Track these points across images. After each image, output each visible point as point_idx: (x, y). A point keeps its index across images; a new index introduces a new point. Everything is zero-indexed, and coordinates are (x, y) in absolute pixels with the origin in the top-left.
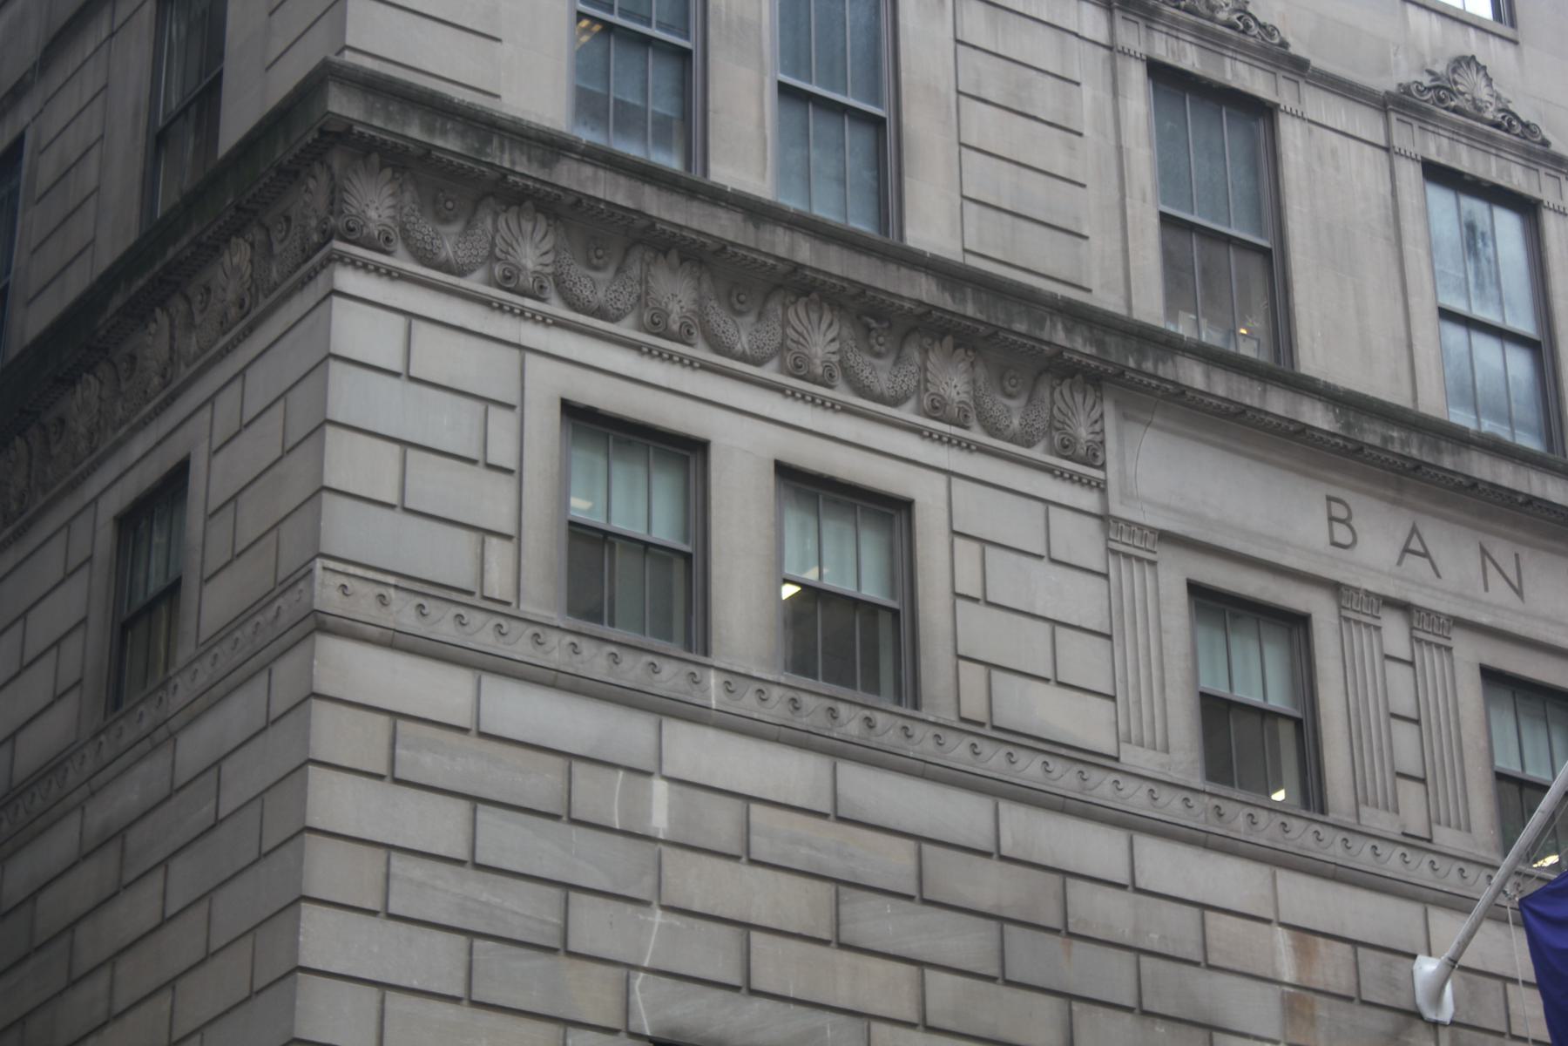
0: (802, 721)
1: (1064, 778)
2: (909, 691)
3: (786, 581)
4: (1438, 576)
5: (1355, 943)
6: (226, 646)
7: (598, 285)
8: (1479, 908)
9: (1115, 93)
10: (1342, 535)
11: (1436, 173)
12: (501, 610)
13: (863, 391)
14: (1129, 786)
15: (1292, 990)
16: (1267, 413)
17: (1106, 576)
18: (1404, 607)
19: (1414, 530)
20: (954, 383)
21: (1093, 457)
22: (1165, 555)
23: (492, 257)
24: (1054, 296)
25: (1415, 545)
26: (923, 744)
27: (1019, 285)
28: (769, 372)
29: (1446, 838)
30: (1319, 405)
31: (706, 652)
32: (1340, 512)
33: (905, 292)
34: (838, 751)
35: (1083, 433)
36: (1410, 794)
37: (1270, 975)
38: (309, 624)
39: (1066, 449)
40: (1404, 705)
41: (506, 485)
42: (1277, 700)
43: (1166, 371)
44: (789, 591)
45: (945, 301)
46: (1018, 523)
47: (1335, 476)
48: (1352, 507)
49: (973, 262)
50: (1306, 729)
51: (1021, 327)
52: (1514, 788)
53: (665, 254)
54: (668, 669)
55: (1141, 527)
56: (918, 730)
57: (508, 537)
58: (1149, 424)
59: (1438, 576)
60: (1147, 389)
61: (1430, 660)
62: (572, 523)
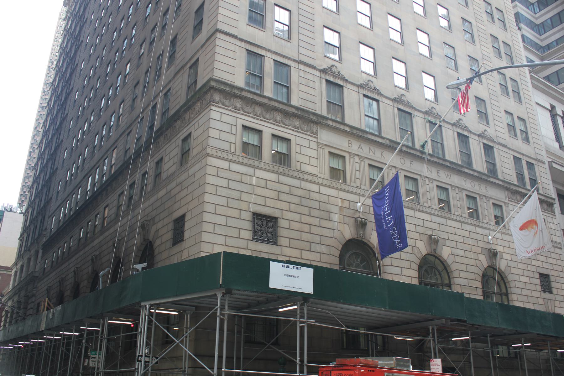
0: (274, 169)
1: (310, 178)
2: (289, 166)
3: (273, 150)
6: (196, 158)
7: (248, 109)
9: (321, 84)
10: (350, 145)
12: (233, 153)
13: (284, 124)
14: (319, 179)
17: (317, 150)
18: (358, 155)
19: (360, 145)
20: (297, 123)
21: (316, 134)
22: (325, 147)
23: (233, 105)
25: (360, 147)
26: (291, 173)
27: (306, 110)
28: (271, 121)
29: (363, 187)
31: (261, 160)
32: (350, 142)
33: (290, 111)
34: (279, 174)
35: (315, 131)
36: (358, 181)
38: (207, 155)
39: (312, 133)
40: (358, 169)
41: (234, 136)
42: (341, 168)
43: (326, 122)
44: (273, 152)
45: (296, 112)
46: (305, 143)
47: (349, 137)
49: (300, 107)
50: (344, 172)
51: (306, 116)
52: (372, 180)
53: (257, 105)
54: (256, 162)
56: (290, 171)
61: (362, 163)
62: (243, 142)
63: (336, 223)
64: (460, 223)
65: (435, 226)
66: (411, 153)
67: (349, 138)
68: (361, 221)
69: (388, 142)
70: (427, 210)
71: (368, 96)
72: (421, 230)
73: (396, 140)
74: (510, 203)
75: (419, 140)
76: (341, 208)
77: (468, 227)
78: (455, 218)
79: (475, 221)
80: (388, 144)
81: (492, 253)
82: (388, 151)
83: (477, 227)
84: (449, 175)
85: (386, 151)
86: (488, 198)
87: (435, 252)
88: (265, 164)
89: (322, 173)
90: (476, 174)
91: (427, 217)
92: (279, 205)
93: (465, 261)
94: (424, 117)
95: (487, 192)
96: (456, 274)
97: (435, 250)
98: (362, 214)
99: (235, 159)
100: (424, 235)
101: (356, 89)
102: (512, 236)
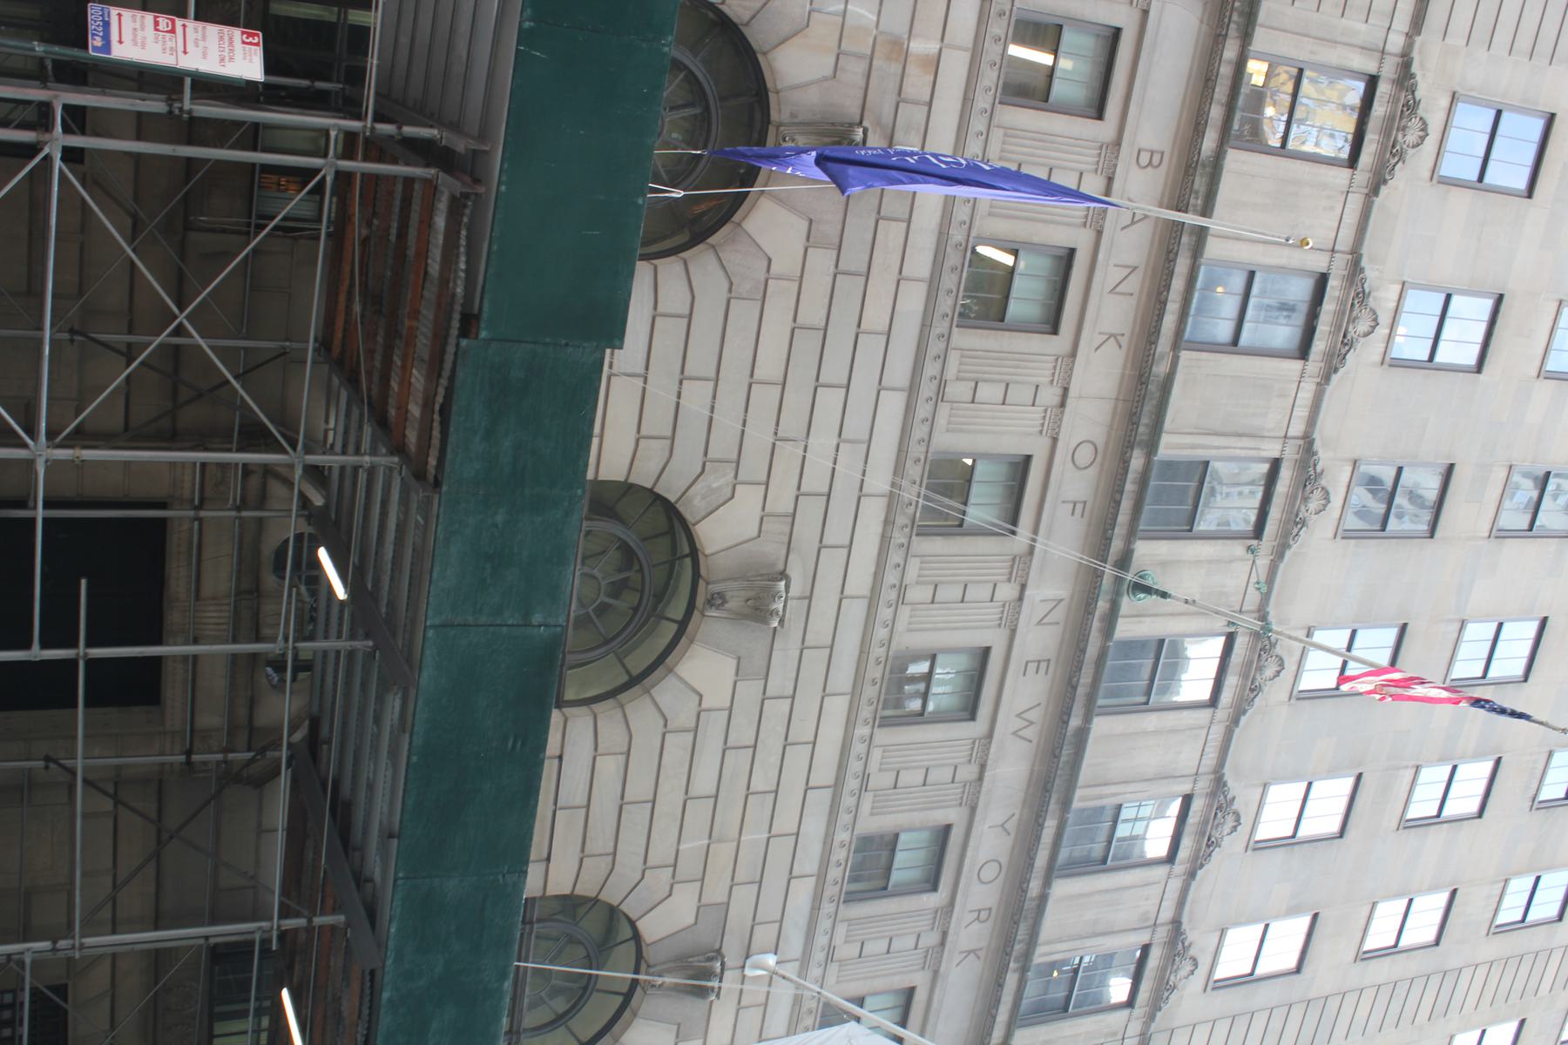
0: (909, 463)
3: (974, 461)
4: (1123, 229)
5: (930, 104)
8: (802, 982)
11: (1276, 464)
14: (929, 407)
15: (905, 46)
16: (1211, 104)
22: (1045, 442)
29: (833, 968)
36: (888, 779)
37: (913, 32)
40: (895, 945)
42: (896, 876)
44: (969, 462)
48: (1087, 471)
59: (1123, 229)
63: (842, 7)
64: (831, 781)
67: (1172, 153)
70: (891, 577)
72: (807, 530)
73: (1122, 617)
75: (1164, 564)
76: (899, 50)
77: (814, 827)
79: (837, 888)
80: (1154, 369)
81: (708, 964)
84: (1028, 733)
86: (933, 961)
87: (710, 602)
88: (925, 443)
89: (964, 367)
90: (1034, 887)
94: (1162, 925)
95: (958, 958)
96: (612, 731)
102: (788, 1035)
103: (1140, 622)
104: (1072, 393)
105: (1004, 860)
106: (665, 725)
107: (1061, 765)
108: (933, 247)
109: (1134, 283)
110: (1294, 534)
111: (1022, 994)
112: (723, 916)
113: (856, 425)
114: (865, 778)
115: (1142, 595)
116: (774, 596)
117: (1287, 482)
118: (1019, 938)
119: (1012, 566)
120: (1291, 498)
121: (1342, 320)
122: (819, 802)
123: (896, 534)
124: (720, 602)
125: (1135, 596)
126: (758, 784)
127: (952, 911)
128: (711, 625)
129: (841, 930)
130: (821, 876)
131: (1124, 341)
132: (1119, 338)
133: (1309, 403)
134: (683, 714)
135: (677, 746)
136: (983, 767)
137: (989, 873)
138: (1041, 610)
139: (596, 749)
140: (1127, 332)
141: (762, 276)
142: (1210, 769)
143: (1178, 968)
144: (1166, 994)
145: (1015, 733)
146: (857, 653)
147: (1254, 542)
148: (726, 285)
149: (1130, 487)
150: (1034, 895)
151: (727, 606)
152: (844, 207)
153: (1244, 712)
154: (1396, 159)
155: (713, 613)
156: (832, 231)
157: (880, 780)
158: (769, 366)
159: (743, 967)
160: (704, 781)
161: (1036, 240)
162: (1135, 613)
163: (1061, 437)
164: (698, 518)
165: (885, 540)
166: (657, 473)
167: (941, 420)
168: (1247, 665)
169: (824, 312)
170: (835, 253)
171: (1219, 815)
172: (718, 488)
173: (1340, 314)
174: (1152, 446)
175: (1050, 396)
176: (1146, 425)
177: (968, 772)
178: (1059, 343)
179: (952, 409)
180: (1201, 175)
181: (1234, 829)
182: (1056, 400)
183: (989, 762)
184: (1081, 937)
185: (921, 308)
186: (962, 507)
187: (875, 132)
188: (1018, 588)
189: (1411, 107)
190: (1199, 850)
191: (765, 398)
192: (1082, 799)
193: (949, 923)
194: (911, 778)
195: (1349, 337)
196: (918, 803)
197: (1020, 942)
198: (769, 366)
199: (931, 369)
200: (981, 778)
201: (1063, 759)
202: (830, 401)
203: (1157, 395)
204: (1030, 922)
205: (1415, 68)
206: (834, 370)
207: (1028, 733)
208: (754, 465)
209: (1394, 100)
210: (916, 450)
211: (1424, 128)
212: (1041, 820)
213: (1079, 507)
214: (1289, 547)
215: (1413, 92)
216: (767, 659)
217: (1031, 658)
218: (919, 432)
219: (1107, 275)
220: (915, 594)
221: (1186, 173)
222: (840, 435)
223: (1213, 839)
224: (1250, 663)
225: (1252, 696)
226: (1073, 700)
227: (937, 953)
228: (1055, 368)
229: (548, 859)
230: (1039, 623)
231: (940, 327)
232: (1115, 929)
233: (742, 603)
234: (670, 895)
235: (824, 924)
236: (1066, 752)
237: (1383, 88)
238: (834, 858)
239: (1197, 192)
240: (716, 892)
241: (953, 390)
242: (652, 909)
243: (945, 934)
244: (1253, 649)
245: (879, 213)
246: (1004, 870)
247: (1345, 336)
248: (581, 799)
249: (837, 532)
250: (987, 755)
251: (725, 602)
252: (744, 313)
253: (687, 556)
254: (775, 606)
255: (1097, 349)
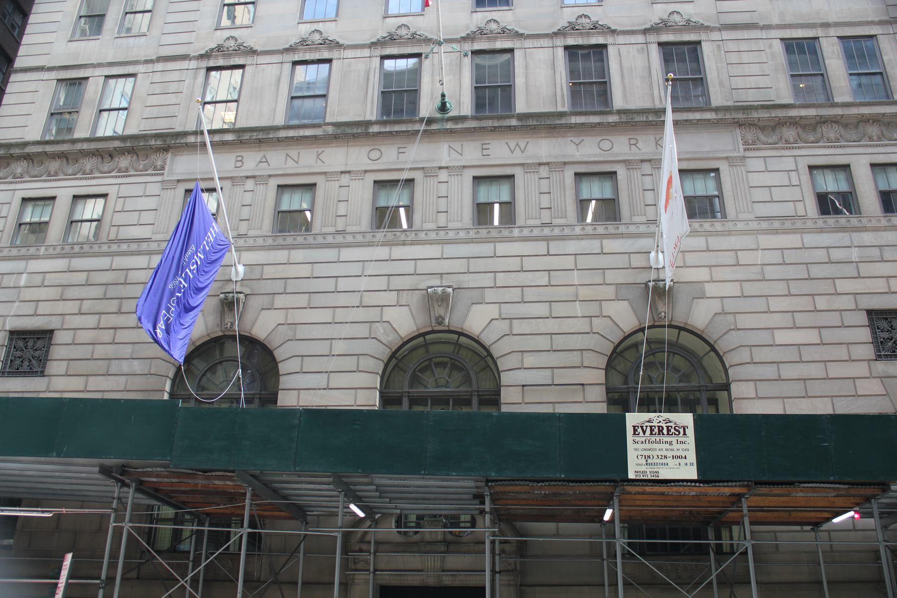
1: (134, 247)
7: (37, 170)
10: (239, 164)
12: (804, 218)
19: (287, 155)
20: (124, 162)
24: (152, 134)
27: (166, 133)
30: (230, 134)
32: (240, 158)
35: (159, 163)
39: (155, 169)
43: (183, 141)
45: (122, 145)
47: (238, 150)
50: (720, 197)
51: (141, 144)
52: (601, 202)
54: (610, 227)
55: (171, 180)
57: (801, 201)
58: (183, 155)
60: (178, 147)
61: (261, 188)
65: (460, 266)
66: (397, 132)
68: (226, 298)
69: (330, 130)
71: (306, 60)
74: (748, 154)
78: (526, 232)
82: (336, 147)
83: (853, 231)
84: (522, 146)
85: (333, 147)
91: (433, 251)
92: (61, 307)
93: (551, 326)
97: (440, 320)
98: (242, 285)
99: (810, 224)
100: (411, 292)
101: (366, 52)
103: (463, 103)
104: (344, 170)
105: (599, 139)
106: (508, 335)
107: (539, 123)
108: (275, 251)
109: (293, 153)
110: (419, 37)
111: (681, 108)
112: (624, 285)
113: (355, 269)
114: (544, 225)
115: (448, 105)
116: (435, 293)
117: (393, 49)
118: (645, 119)
119: (429, 176)
120: (401, 44)
121: (314, 48)
122: (555, 247)
123: (410, 238)
124: (440, 319)
125: (449, 109)
126: (545, 281)
127: (628, 160)
128: (453, 320)
129: (636, 219)
130: (708, 234)
131: (320, 150)
132: (319, 153)
133: (353, 51)
134: (503, 326)
135: (518, 327)
136: (540, 164)
137: (606, 145)
138: (454, 155)
139: (520, 368)
140: (316, 150)
141: (285, 327)
142: (550, 41)
143: (675, 22)
144: (692, 24)
145: (523, 152)
146: (472, 244)
147: (423, 56)
148: (289, 342)
149: (388, 129)
150: (618, 118)
151: (442, 314)
152: (257, 296)
153: (517, 32)
154: (241, 47)
155: (447, 321)
156: (266, 299)
157: (546, 217)
158: (325, 316)
159: (658, 269)
160: (542, 309)
161: (273, 204)
162: (458, 107)
163: (364, 169)
164: (398, 337)
165: (413, 243)
166: (375, 359)
167: (355, 229)
168: (489, 39)
169: (302, 295)
170: (276, 296)
171: (577, 28)
172: (384, 329)
173: (310, 50)
174: (369, 123)
175: (345, 180)
176: (357, 130)
177: (544, 171)
178: (319, 180)
179: (425, 222)
180: (244, 136)
181: (586, 16)
182: (347, 175)
183: (538, 161)
184: (651, 84)
185: (301, 251)
186: (390, 209)
187: (225, 288)
188: (442, 170)
189: (219, 48)
190: (598, 32)
191: (341, 315)
192: (563, 106)
193: (635, 160)
194: (545, 201)
195: (321, 42)
196: (561, 193)
197: (647, 118)
198: (325, 316)
199: (330, 239)
200: (548, 164)
201: (535, 123)
202: (343, 284)
203: (343, 128)
204: (635, 115)
205: (203, 52)
206: (329, 285)
207: (522, 146)
208: (373, 314)
209: (216, 57)
210: (472, 234)
211: (228, 39)
212: (573, 125)
213: (401, 150)
214: (426, 37)
215: (213, 49)
216: (473, 290)
217: (481, 154)
218: (359, 238)
219: (290, 167)
220: (442, 223)
221: (244, 143)
222: (361, 276)
223: (592, 27)
224: (489, 38)
225: (507, 31)
226: (501, 127)
227: (655, 162)
228: (331, 180)
229: (583, 385)
230: (461, 155)
231: (310, 240)
232: (647, 65)
233: (441, 308)
234: (609, 316)
235: (632, 229)
236: (531, 122)
237: (212, 64)
238: (591, 232)
239: (251, 136)
240: (610, 292)
241: (340, 226)
242: (618, 325)
243: (642, 161)
244: (481, 39)
245: (259, 279)
246: (605, 137)
247: (321, 44)
248: (548, 372)
249: (408, 267)
250: (533, 164)
251: (440, 316)
252: (302, 332)
253: (425, 339)
254: (440, 292)
255: (324, 163)
